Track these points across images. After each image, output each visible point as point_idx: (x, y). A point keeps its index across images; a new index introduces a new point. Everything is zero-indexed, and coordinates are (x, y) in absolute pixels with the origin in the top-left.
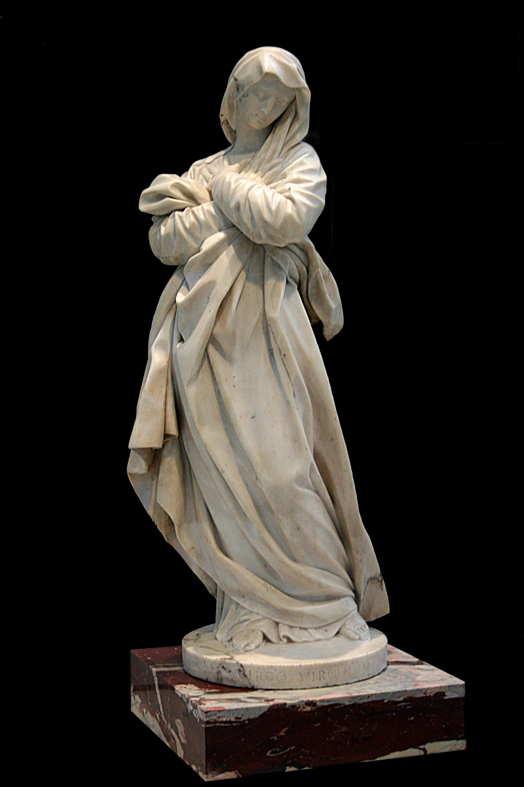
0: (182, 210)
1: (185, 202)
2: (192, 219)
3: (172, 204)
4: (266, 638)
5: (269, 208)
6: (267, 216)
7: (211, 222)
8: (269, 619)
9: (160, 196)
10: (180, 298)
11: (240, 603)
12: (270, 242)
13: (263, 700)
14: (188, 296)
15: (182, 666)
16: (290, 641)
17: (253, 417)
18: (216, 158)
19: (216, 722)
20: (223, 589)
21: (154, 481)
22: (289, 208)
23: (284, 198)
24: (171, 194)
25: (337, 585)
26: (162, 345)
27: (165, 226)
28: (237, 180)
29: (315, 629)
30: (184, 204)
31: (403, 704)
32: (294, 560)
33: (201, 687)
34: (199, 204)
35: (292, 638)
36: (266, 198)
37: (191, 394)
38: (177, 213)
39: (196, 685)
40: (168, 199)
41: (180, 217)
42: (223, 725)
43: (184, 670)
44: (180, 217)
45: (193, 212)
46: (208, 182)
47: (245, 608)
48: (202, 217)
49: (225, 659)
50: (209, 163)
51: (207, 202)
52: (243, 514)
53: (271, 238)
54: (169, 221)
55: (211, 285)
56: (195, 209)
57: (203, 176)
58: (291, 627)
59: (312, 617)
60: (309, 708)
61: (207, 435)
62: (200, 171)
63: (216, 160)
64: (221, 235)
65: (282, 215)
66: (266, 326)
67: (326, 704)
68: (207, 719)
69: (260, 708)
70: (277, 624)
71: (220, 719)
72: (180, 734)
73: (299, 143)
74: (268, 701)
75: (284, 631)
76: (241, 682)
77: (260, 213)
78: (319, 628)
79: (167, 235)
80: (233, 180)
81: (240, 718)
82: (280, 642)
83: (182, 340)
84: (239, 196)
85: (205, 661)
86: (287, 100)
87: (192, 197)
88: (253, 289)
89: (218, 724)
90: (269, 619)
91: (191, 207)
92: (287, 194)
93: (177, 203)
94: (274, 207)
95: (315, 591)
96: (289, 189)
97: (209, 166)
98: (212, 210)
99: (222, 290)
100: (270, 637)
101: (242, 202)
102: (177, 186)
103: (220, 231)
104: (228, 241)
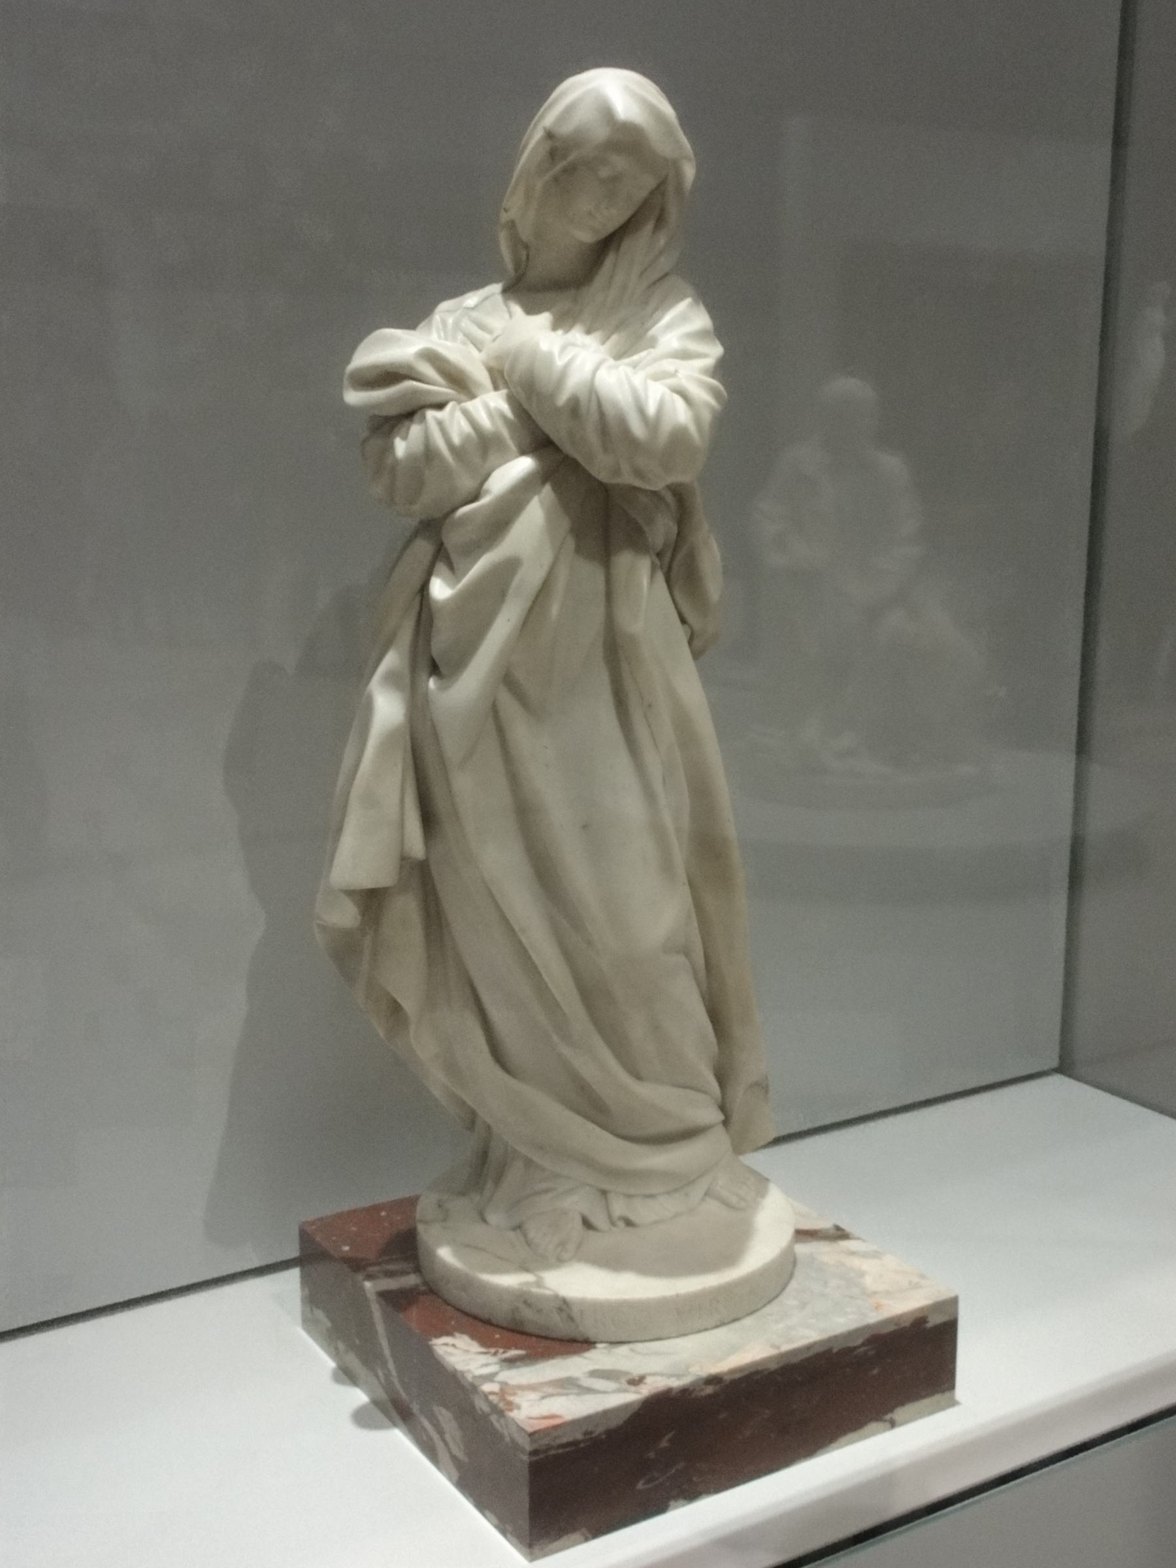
0: (440, 406)
1: (441, 389)
2: (466, 427)
3: (415, 392)
4: (587, 1224)
5: (641, 411)
6: (637, 429)
7: (505, 433)
8: (590, 1185)
9: (389, 376)
10: (440, 590)
11: (535, 1158)
12: (637, 483)
13: (623, 1381)
14: (460, 586)
15: (418, 1270)
16: (629, 1223)
17: (585, 827)
18: (486, 298)
19: (549, 1448)
20: (489, 1121)
21: (369, 937)
22: (681, 414)
23: (668, 392)
24: (419, 373)
25: (709, 1115)
26: (392, 679)
27: (405, 438)
28: (563, 349)
29: (669, 1193)
30: (446, 394)
31: (862, 1349)
32: (638, 1077)
33: (486, 1343)
34: (472, 396)
35: (633, 1218)
36: (634, 392)
37: (472, 791)
38: (431, 414)
39: (473, 1337)
40: (415, 383)
41: (440, 424)
42: (561, 1451)
43: (425, 1283)
44: (440, 424)
45: (466, 414)
46: (480, 350)
47: (543, 1170)
48: (486, 422)
49: (528, 1283)
50: (473, 309)
51: (488, 391)
52: (551, 1005)
53: (638, 473)
54: (415, 430)
55: (511, 566)
56: (469, 405)
57: (465, 335)
58: (629, 1196)
59: (665, 1175)
60: (710, 1390)
61: (493, 859)
62: (457, 325)
63: (487, 303)
64: (523, 465)
65: (666, 428)
66: (615, 650)
67: (738, 1376)
68: (535, 1446)
69: (626, 1406)
70: (604, 1193)
71: (558, 1442)
72: (447, 1437)
73: (666, 275)
74: (637, 1381)
75: (619, 1208)
76: (561, 1327)
77: (622, 422)
78: (676, 1190)
79: (411, 458)
80: (556, 350)
81: (591, 1433)
82: (614, 1229)
83: (435, 669)
84: (574, 383)
85: (484, 1286)
86: (649, 182)
87: (459, 382)
88: (591, 574)
89: (553, 1452)
90: (590, 1185)
91: (459, 402)
92: (671, 381)
93: (429, 392)
94: (651, 410)
95: (671, 1126)
96: (676, 371)
97: (474, 314)
98: (505, 407)
99: (530, 577)
100: (593, 1220)
101: (583, 398)
102: (431, 357)
103: (523, 452)
104: (543, 476)
